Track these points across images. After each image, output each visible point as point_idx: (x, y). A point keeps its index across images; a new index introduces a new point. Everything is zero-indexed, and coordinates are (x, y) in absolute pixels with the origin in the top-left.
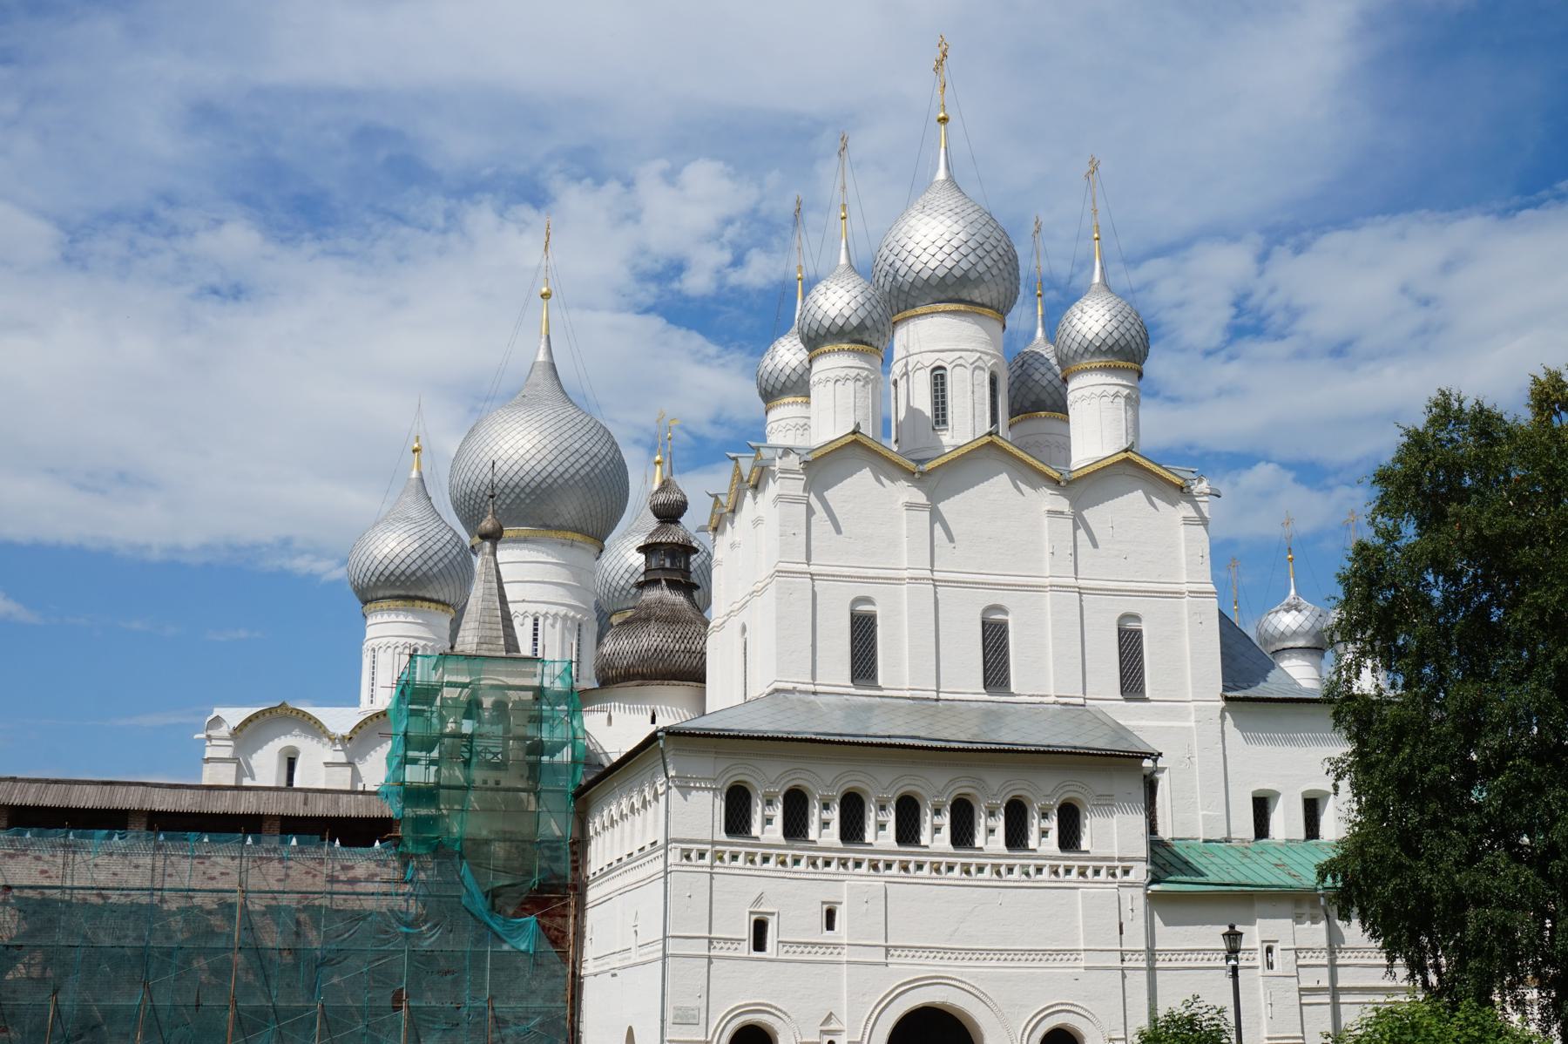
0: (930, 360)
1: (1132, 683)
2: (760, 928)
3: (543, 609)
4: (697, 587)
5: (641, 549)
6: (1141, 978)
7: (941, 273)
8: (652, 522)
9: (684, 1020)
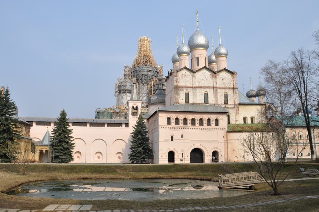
0: (197, 56)
2: (172, 137)
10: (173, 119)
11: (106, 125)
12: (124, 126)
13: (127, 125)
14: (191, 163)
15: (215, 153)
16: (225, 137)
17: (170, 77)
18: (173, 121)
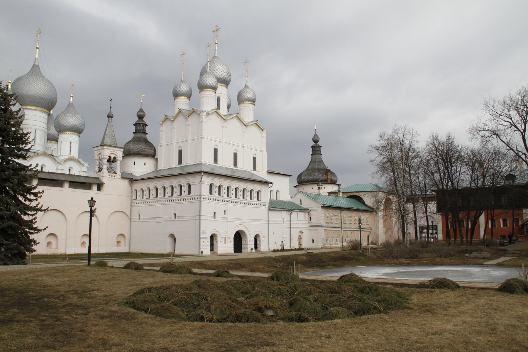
1: (254, 168)
3: (37, 127)
4: (147, 134)
5: (134, 125)
6: (267, 225)
7: (221, 77)
8: (137, 119)
9: (204, 233)
10: (216, 186)
11: (66, 185)
12: (95, 188)
13: (100, 187)
14: (235, 252)
15: (256, 238)
16: (267, 215)
17: (181, 119)
18: (215, 190)
